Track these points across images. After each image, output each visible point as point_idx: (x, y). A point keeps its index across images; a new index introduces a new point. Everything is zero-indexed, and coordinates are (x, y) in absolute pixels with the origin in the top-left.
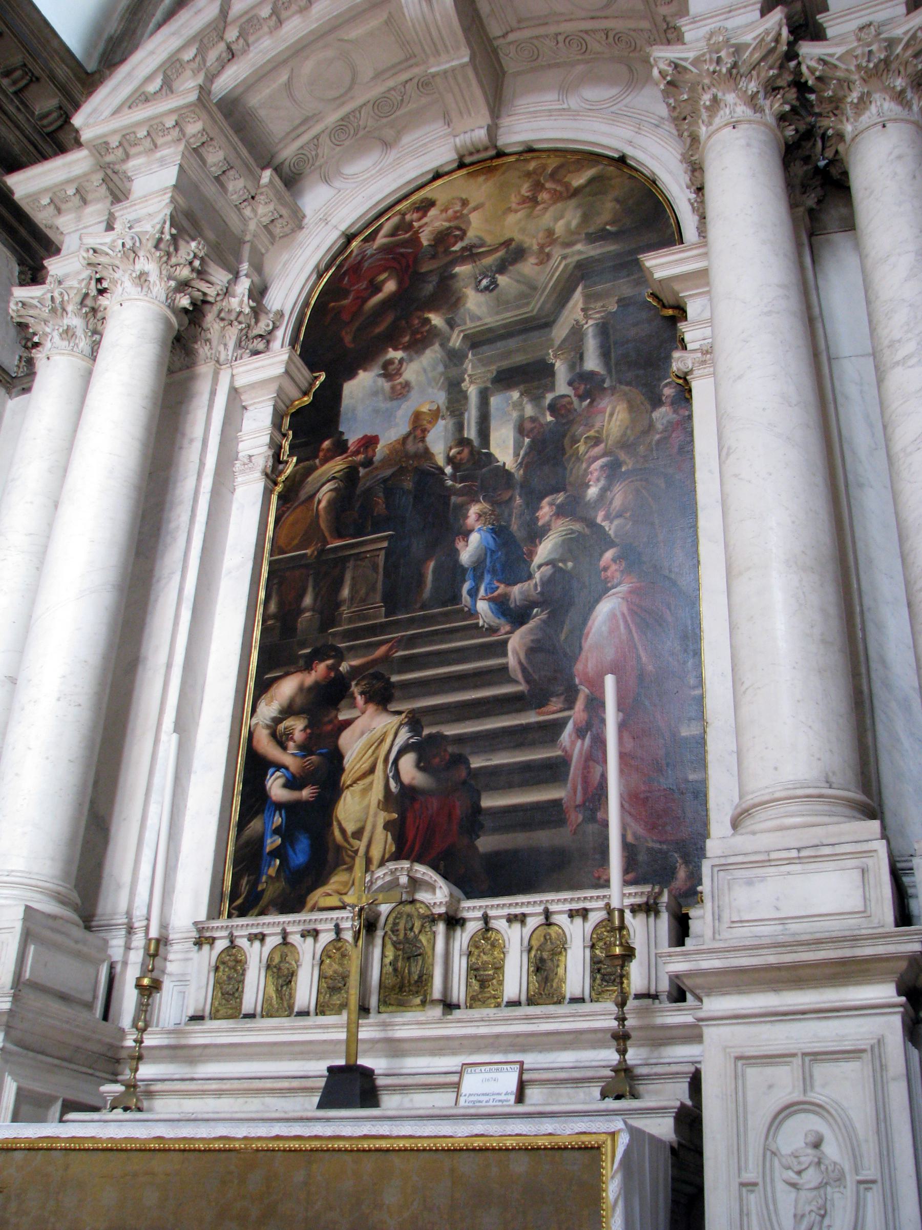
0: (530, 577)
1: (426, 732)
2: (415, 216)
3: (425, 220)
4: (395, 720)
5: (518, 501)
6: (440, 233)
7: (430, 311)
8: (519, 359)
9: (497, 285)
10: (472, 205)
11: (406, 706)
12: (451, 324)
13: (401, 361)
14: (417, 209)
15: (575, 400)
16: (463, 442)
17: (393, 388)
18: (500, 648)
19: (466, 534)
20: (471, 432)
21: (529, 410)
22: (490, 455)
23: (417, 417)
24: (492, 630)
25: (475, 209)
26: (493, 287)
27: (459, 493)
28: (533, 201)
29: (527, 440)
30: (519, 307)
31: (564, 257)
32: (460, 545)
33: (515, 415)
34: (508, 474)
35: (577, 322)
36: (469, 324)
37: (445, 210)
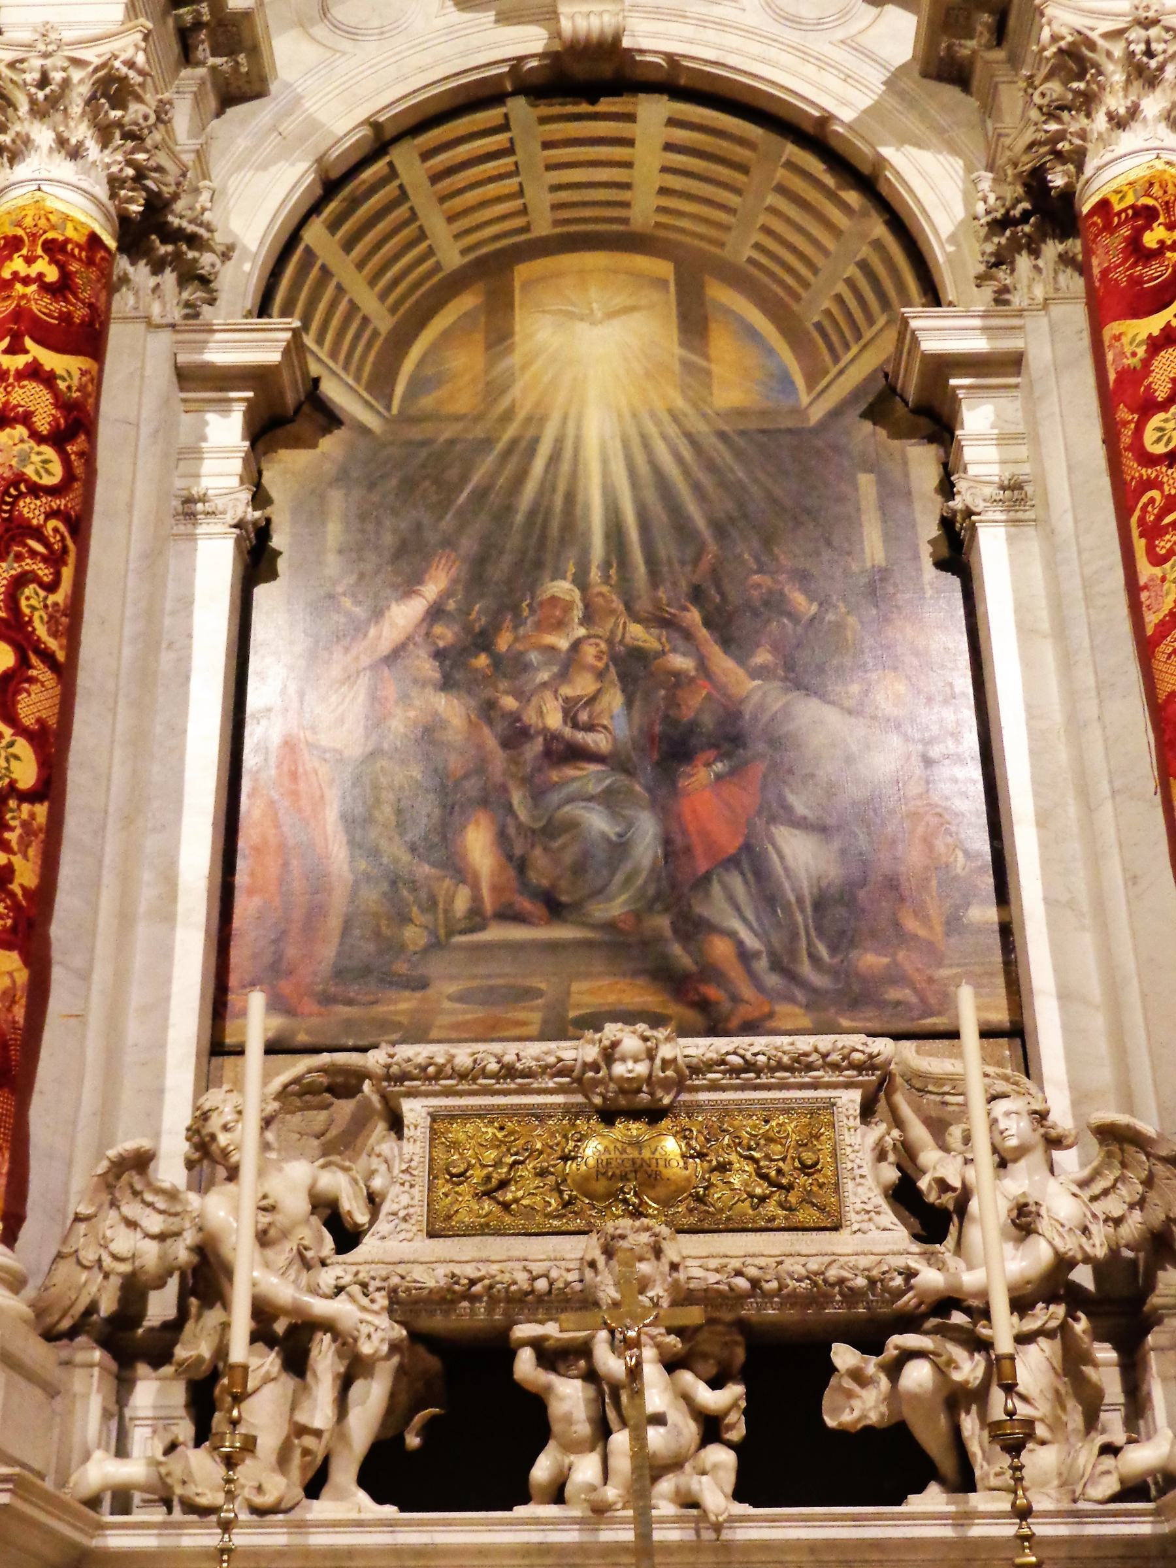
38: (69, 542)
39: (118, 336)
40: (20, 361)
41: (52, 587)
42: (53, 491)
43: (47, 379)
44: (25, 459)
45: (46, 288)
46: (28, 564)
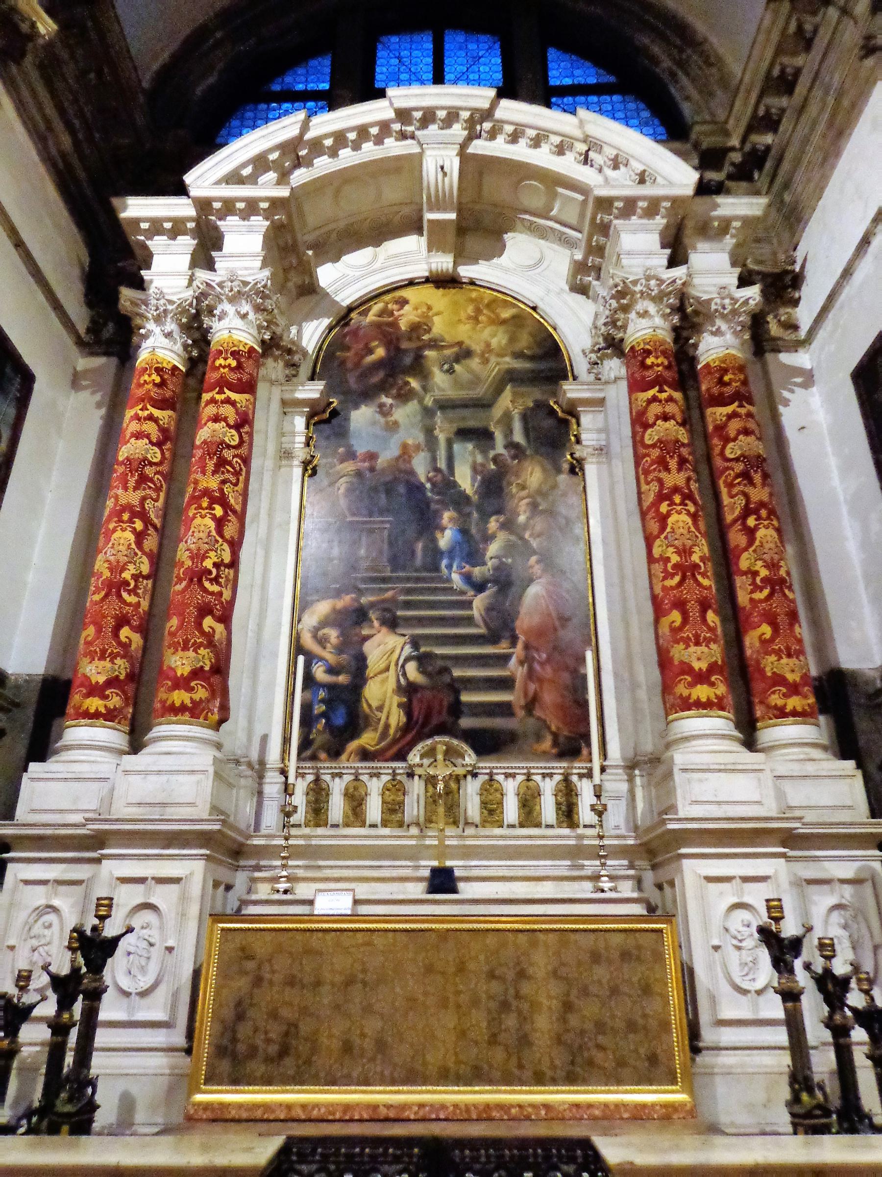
0: (484, 564)
1: (422, 650)
2: (395, 307)
3: (401, 312)
4: (402, 640)
5: (475, 515)
6: (413, 324)
7: (410, 375)
8: (471, 424)
9: (454, 371)
10: (435, 310)
11: (409, 632)
12: (425, 389)
13: (391, 405)
14: (396, 302)
15: (509, 460)
16: (437, 470)
17: (387, 423)
18: (468, 605)
19: (443, 529)
20: (442, 464)
21: (479, 459)
22: (455, 482)
23: (405, 447)
24: (463, 593)
25: (437, 314)
26: (451, 371)
27: (438, 502)
28: (475, 319)
29: (479, 478)
30: (469, 389)
31: (498, 364)
32: (438, 535)
33: (470, 459)
34: (467, 498)
35: (508, 408)
36: (437, 392)
37: (416, 309)
38: (242, 466)
39: (262, 389)
40: (223, 397)
41: (236, 485)
42: (234, 447)
43: (233, 403)
44: (225, 434)
45: (232, 369)
46: (227, 476)
